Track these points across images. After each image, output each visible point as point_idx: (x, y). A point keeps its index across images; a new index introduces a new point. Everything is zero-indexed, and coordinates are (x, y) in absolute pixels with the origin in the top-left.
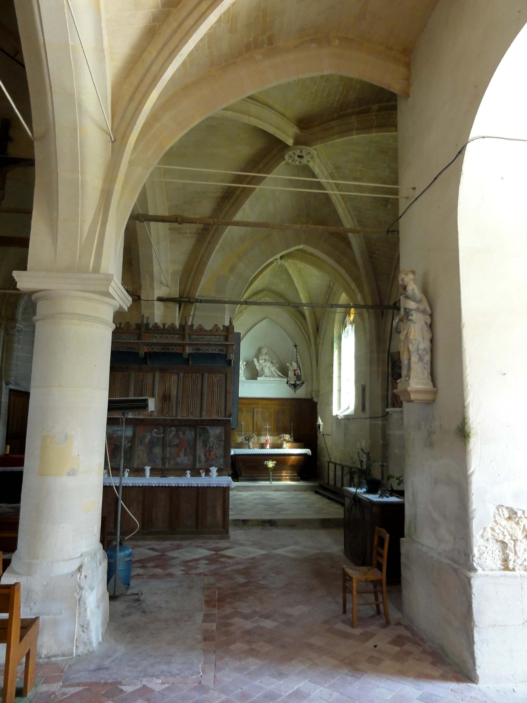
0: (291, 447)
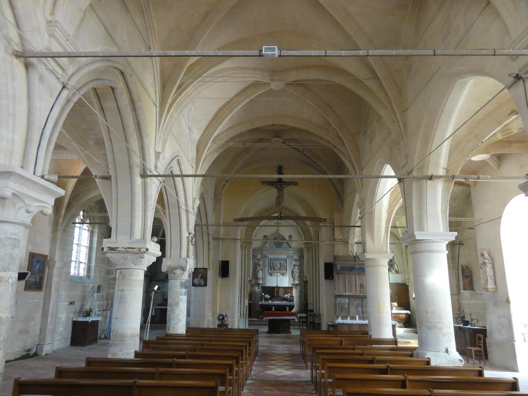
0: (396, 310)
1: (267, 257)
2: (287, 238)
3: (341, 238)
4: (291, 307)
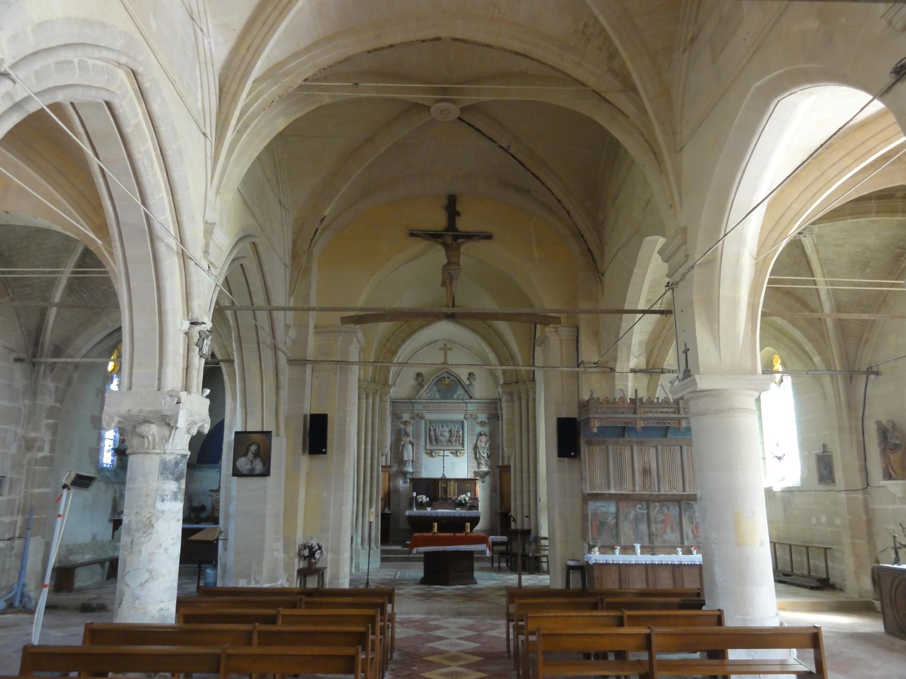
1: (422, 418)
3: (596, 359)
4: (475, 521)
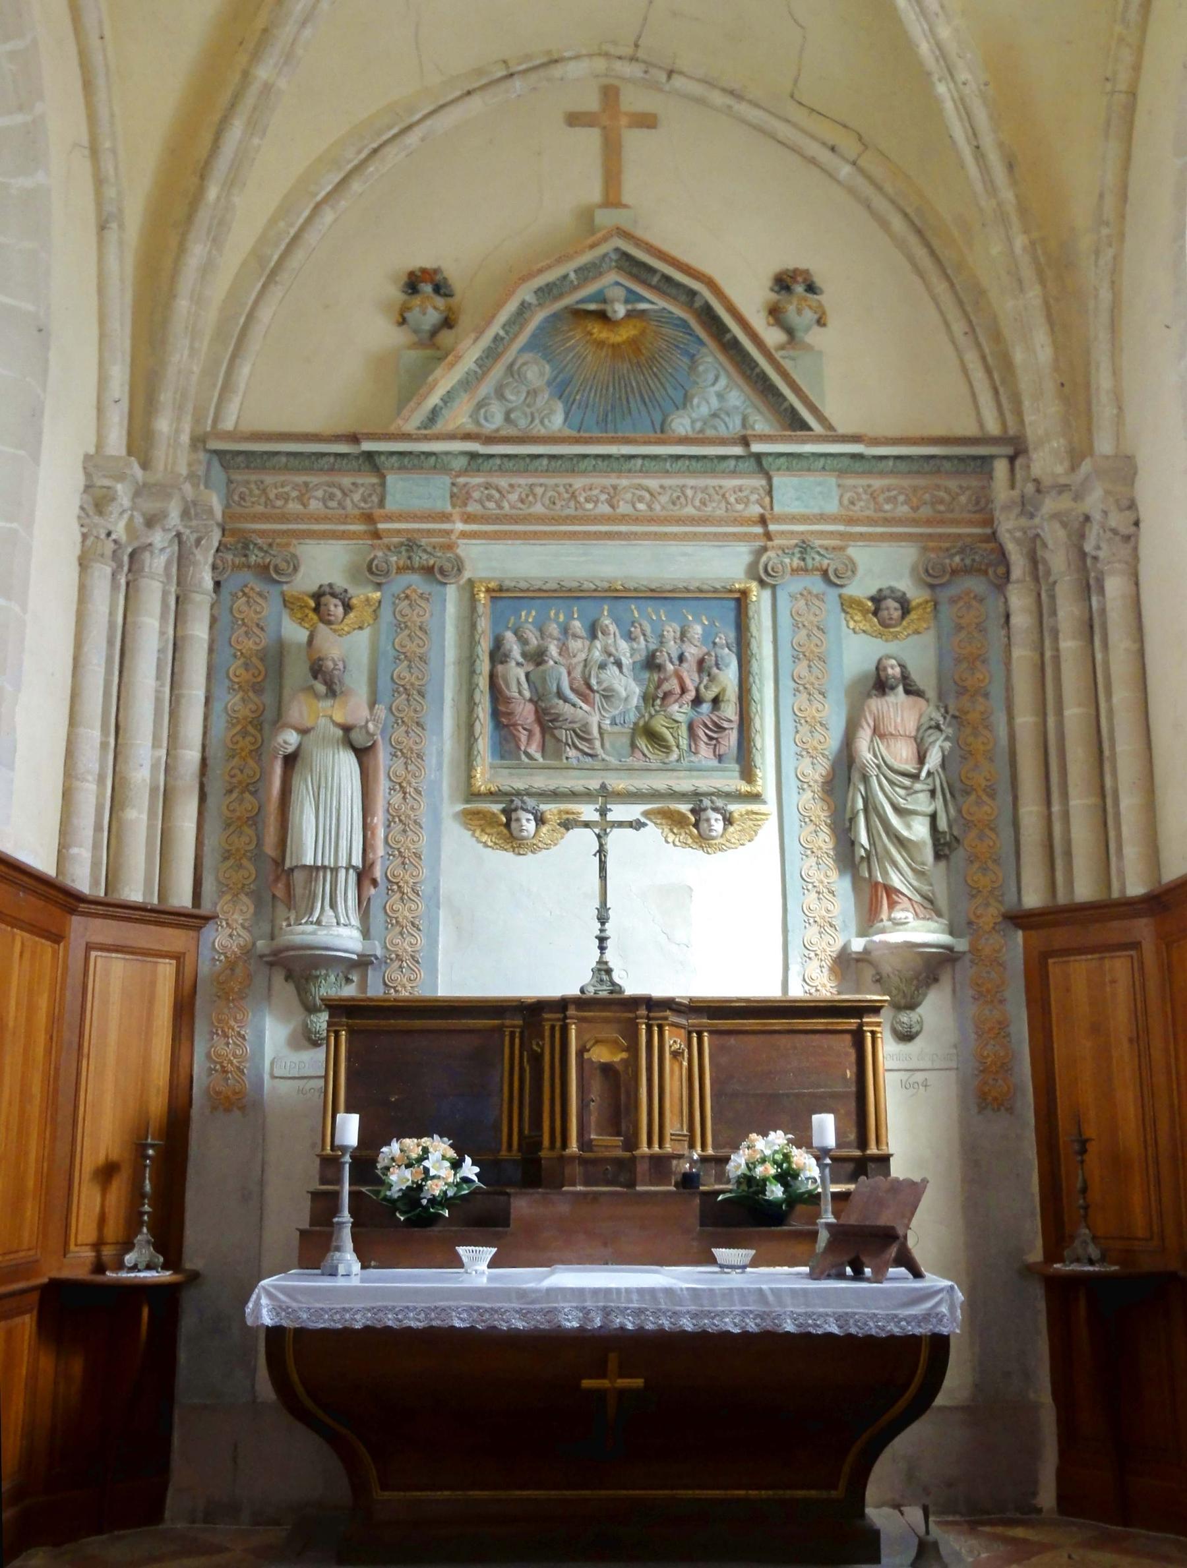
2: (749, 295)
